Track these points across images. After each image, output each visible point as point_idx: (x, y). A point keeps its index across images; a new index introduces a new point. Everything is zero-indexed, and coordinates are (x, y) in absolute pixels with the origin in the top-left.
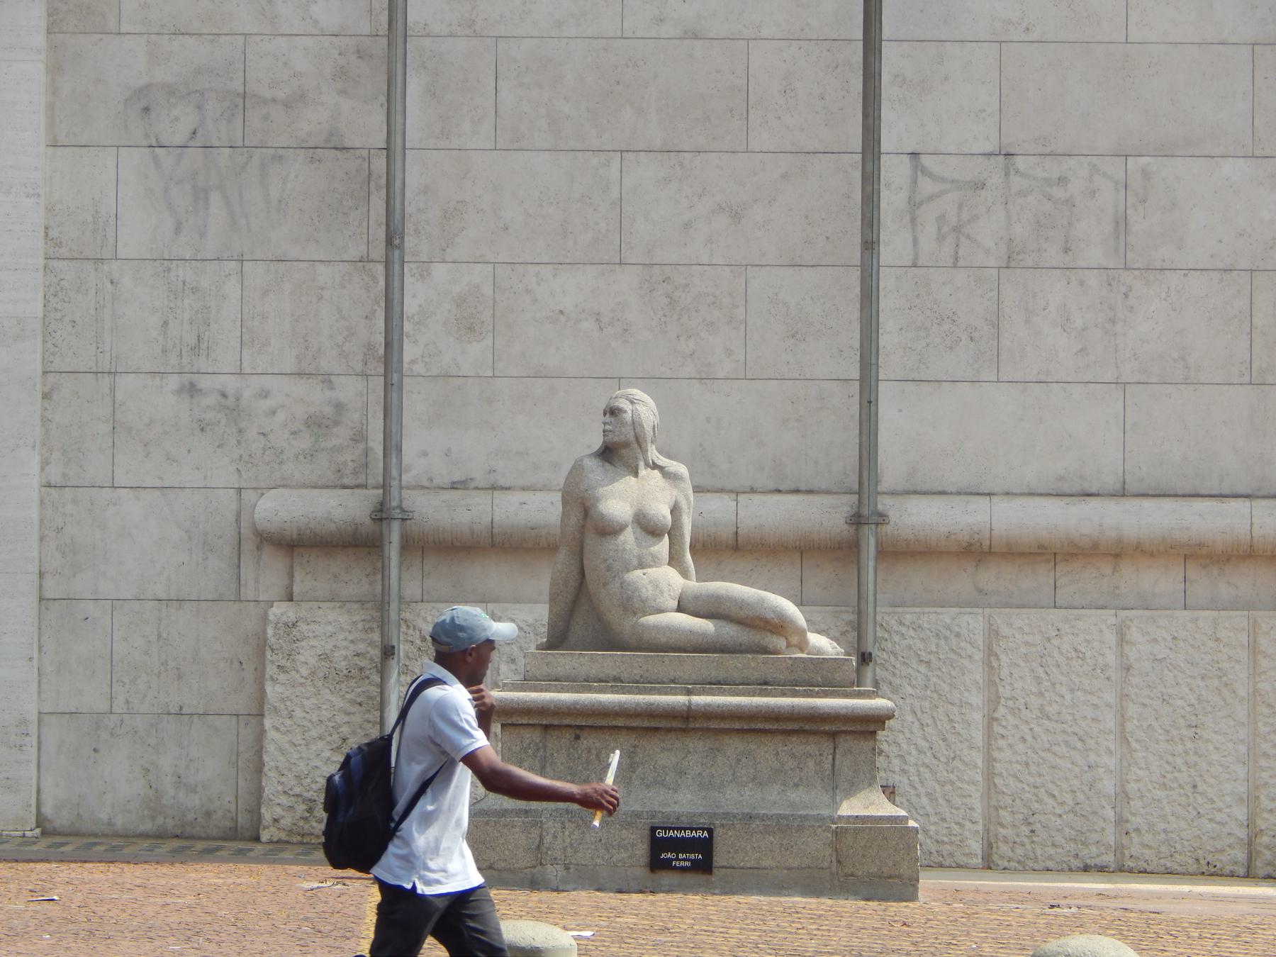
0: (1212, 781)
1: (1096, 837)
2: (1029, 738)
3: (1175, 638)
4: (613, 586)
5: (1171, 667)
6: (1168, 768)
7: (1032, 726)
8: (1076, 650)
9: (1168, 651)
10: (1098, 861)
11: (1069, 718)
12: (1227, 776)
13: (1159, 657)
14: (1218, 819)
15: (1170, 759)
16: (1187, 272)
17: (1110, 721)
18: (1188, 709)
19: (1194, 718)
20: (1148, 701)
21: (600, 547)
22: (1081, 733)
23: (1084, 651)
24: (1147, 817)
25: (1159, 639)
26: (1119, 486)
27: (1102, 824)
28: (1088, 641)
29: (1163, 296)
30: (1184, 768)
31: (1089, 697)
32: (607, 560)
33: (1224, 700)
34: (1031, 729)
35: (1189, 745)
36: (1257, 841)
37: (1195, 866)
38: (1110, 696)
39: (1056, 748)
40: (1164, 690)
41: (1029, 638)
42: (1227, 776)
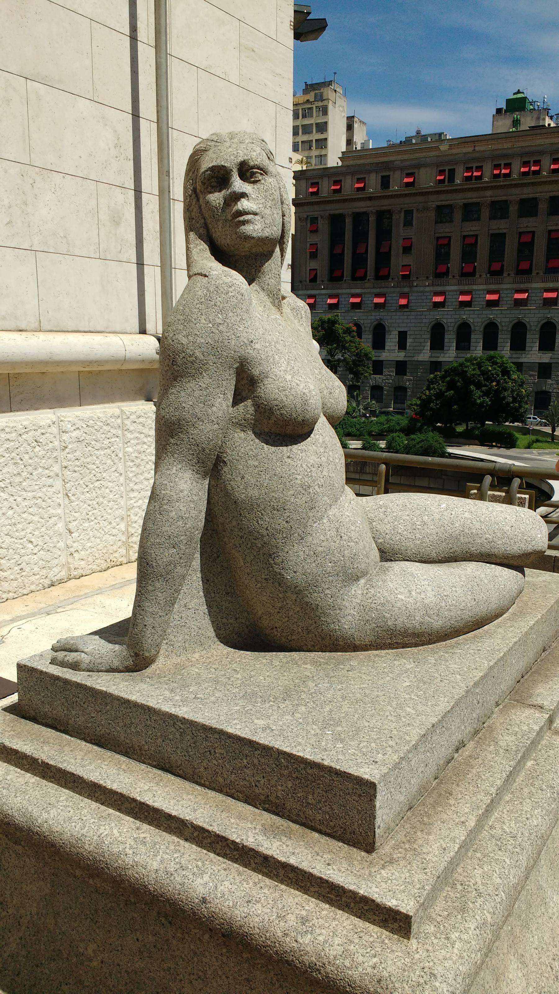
0: (110, 511)
1: (56, 562)
2: (15, 507)
3: (88, 426)
4: (322, 537)
5: (87, 445)
6: (89, 508)
7: (16, 497)
8: (36, 441)
9: (84, 435)
10: (58, 577)
11: (37, 487)
12: (117, 507)
13: (81, 440)
14: (114, 533)
15: (90, 503)
16: (64, 175)
17: (58, 484)
18: (97, 470)
19: (100, 475)
20: (76, 469)
21: (289, 460)
22: (43, 496)
23: (41, 441)
24: (81, 542)
25: (80, 428)
26: (37, 324)
27: (60, 553)
28: (43, 434)
29: (53, 190)
30: (97, 506)
31: (47, 471)
32: (309, 487)
33: (113, 461)
34: (15, 500)
35: (99, 492)
36: (130, 541)
37: (105, 564)
38: (56, 468)
39: (31, 510)
40: (85, 460)
41: (8, 436)
42: (117, 507)
